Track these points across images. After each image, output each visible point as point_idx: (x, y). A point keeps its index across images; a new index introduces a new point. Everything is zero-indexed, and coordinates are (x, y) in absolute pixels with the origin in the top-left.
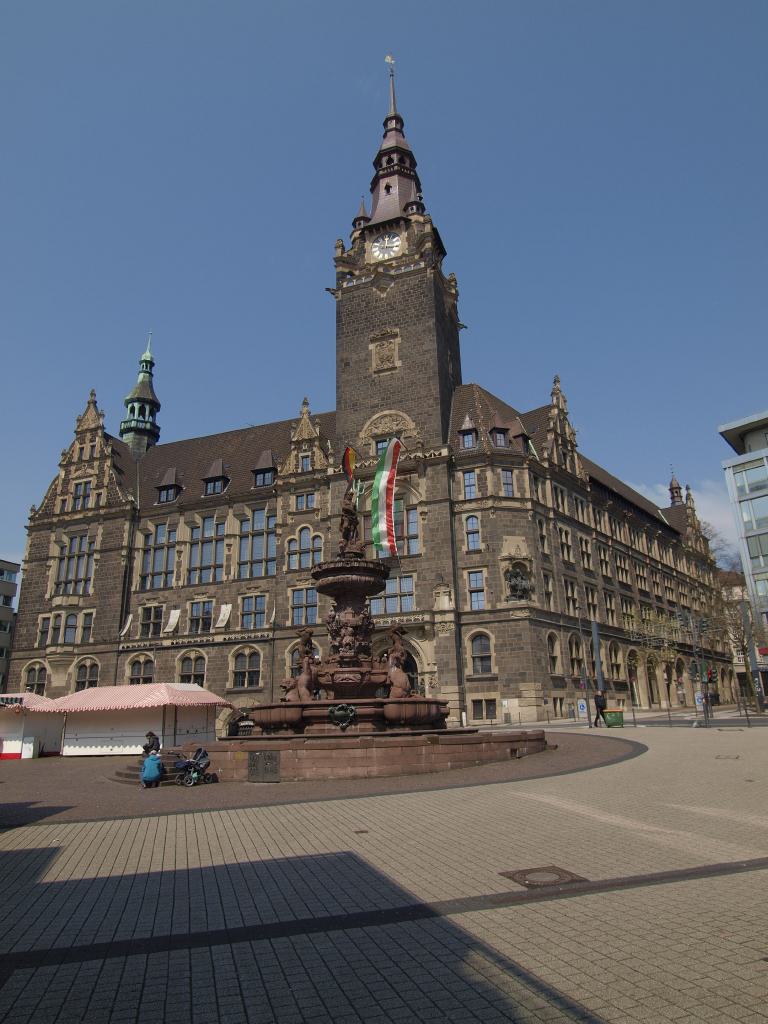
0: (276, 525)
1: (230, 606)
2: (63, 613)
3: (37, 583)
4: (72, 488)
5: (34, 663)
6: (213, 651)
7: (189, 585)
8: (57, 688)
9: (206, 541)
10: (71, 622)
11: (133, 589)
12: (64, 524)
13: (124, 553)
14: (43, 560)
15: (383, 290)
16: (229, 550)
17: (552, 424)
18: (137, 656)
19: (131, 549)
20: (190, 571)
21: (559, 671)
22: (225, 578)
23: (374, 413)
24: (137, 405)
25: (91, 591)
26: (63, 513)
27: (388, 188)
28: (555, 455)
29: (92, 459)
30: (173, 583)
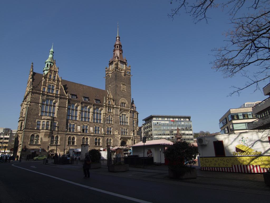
3: (35, 110)
8: (44, 142)
23: (122, 98)
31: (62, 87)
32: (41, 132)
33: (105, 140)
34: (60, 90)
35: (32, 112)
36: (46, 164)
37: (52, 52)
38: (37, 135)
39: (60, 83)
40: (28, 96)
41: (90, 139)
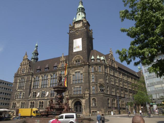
0: (57, 77)
1: (48, 92)
2: (19, 93)
4: (22, 69)
6: (45, 101)
7: (41, 88)
9: (45, 80)
10: (20, 94)
11: (31, 88)
12: (20, 76)
13: (30, 82)
14: (16, 83)
15: (77, 33)
17: (110, 57)
19: (31, 81)
20: (42, 85)
21: (110, 106)
22: (48, 87)
24: (34, 54)
25: (24, 89)
26: (20, 74)
27: (79, 14)
28: (110, 63)
29: (26, 64)
30: (39, 87)
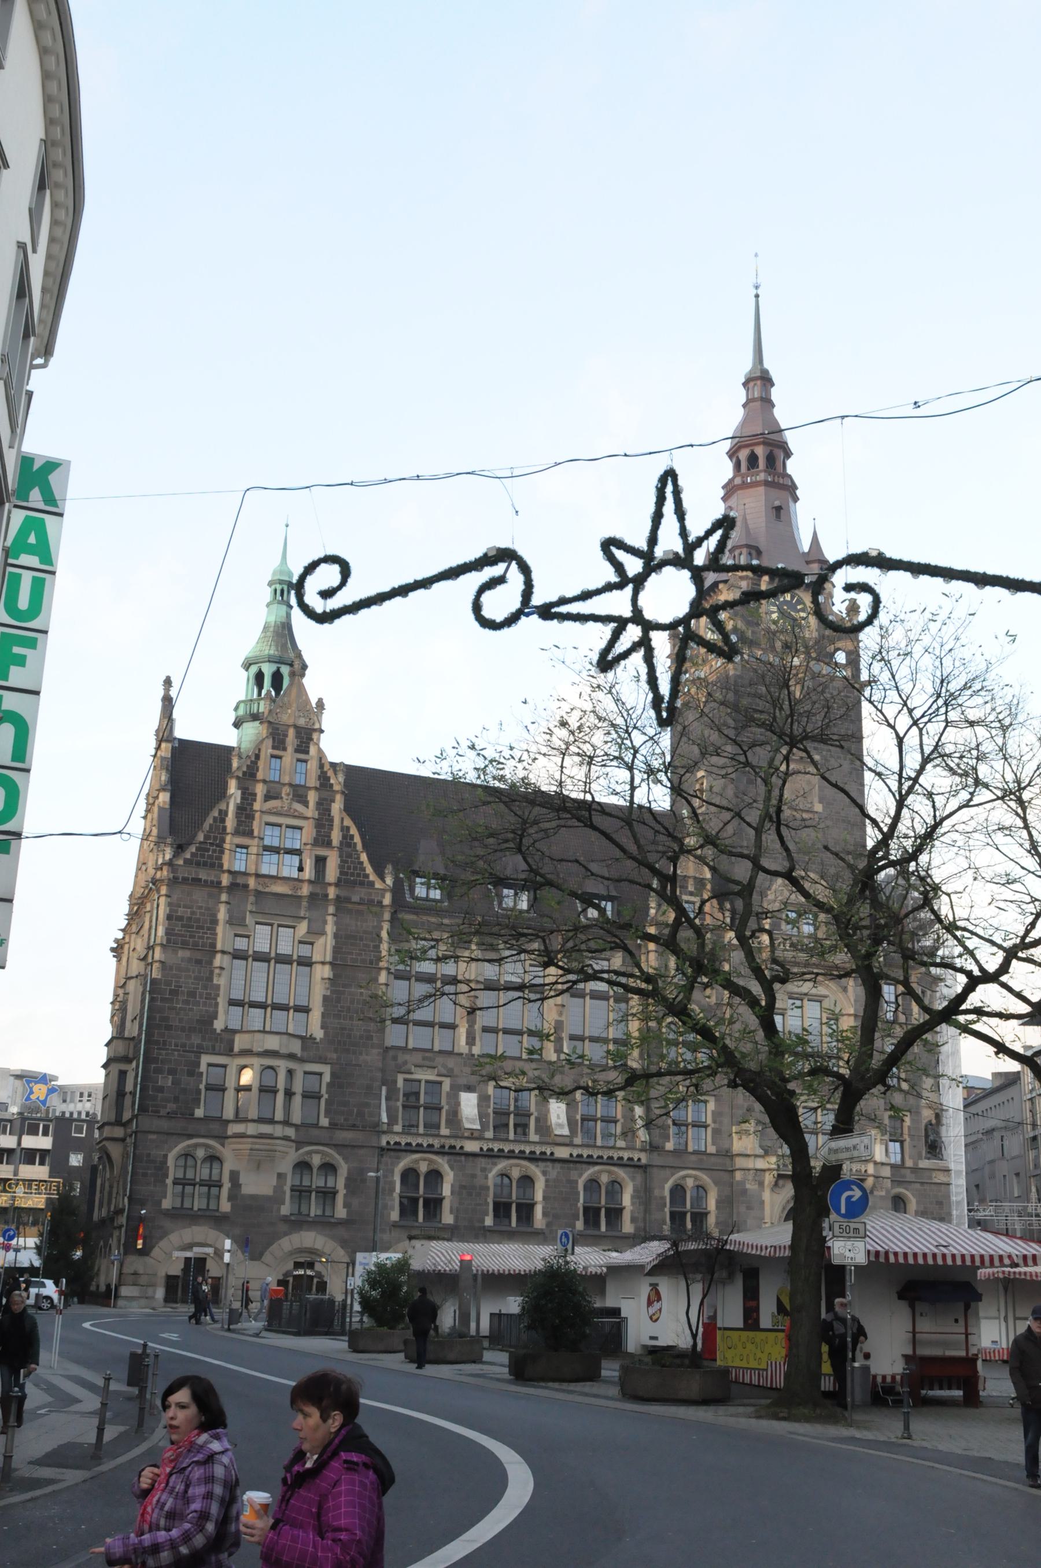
3: (192, 994)
5: (196, 1146)
6: (554, 1171)
16: (561, 1014)
18: (417, 1161)
31: (348, 828)
32: (229, 1133)
33: (657, 1192)
34: (340, 849)
35: (175, 1008)
36: (229, 1330)
37: (285, 588)
38: (211, 1152)
39: (337, 807)
40: (148, 907)
41: (547, 1186)
